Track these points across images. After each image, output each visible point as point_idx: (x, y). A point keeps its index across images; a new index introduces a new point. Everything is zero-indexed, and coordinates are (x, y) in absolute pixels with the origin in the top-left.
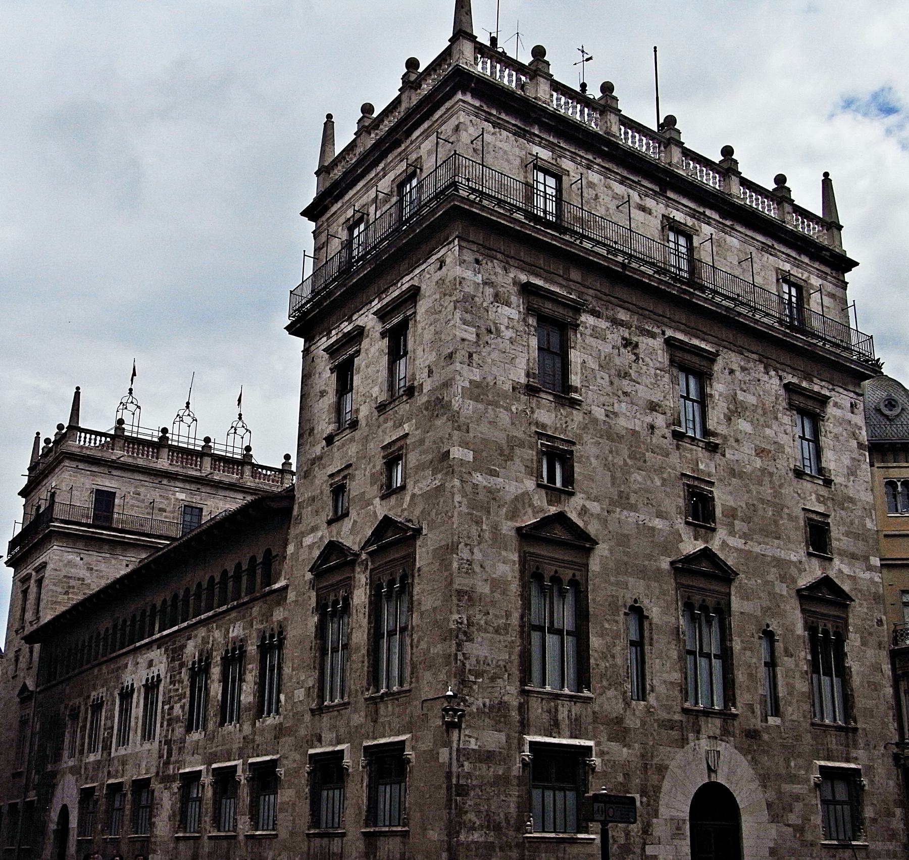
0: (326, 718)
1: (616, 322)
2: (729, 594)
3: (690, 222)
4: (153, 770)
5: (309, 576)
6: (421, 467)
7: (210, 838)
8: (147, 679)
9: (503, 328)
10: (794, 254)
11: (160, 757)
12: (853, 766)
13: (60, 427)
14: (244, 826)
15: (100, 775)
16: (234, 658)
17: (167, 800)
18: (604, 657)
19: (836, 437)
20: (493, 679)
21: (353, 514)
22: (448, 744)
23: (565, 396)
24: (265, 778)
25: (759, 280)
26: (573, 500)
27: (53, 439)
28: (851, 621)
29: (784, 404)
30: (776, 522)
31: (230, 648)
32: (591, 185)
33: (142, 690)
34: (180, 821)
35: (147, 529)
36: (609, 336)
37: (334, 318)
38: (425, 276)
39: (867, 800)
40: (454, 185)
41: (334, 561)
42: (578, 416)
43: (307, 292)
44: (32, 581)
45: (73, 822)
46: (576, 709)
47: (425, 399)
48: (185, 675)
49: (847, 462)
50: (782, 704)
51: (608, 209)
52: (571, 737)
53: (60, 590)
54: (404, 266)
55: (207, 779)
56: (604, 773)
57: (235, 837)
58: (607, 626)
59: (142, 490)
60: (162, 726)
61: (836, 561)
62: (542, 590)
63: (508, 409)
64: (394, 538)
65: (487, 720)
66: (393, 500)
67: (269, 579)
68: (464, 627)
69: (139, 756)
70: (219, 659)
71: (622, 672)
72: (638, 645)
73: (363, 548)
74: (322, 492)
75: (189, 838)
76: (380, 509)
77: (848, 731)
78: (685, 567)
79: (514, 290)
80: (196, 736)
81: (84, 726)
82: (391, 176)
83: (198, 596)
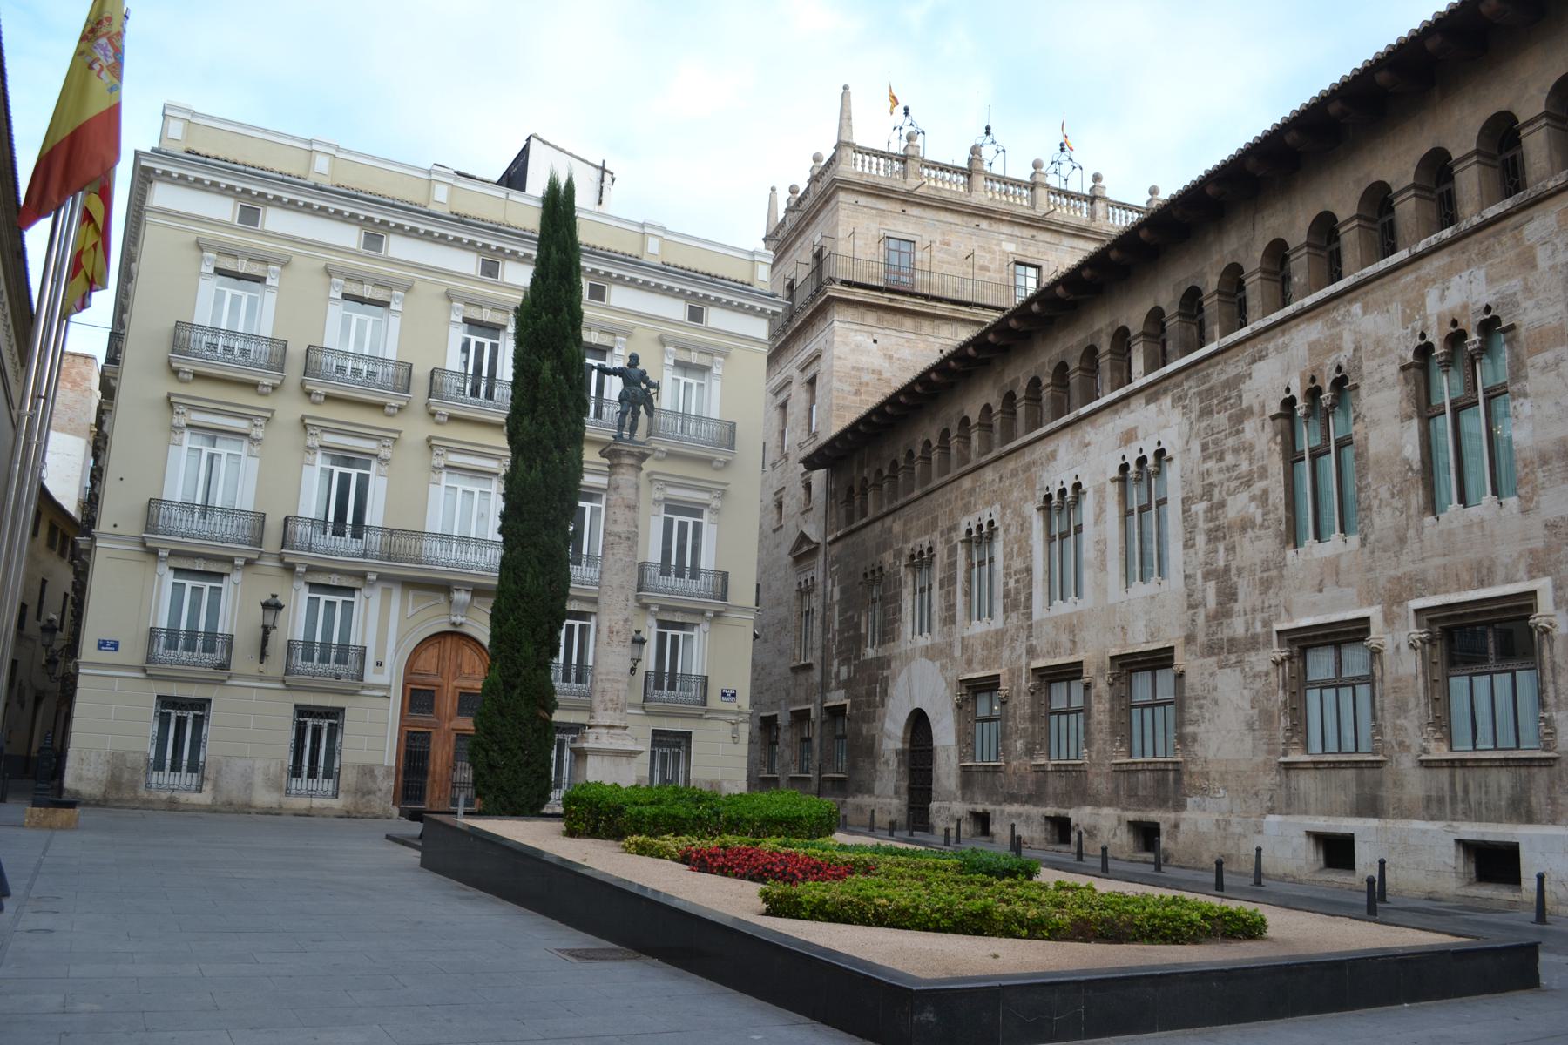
7: (1427, 765)
8: (1124, 468)
11: (1191, 607)
13: (817, 158)
15: (1006, 653)
27: (803, 187)
31: (1435, 338)
33: (1113, 491)
34: (1293, 728)
44: (794, 387)
45: (944, 734)
53: (847, 388)
60: (1188, 544)
69: (1109, 609)
70: (1391, 371)
81: (949, 581)
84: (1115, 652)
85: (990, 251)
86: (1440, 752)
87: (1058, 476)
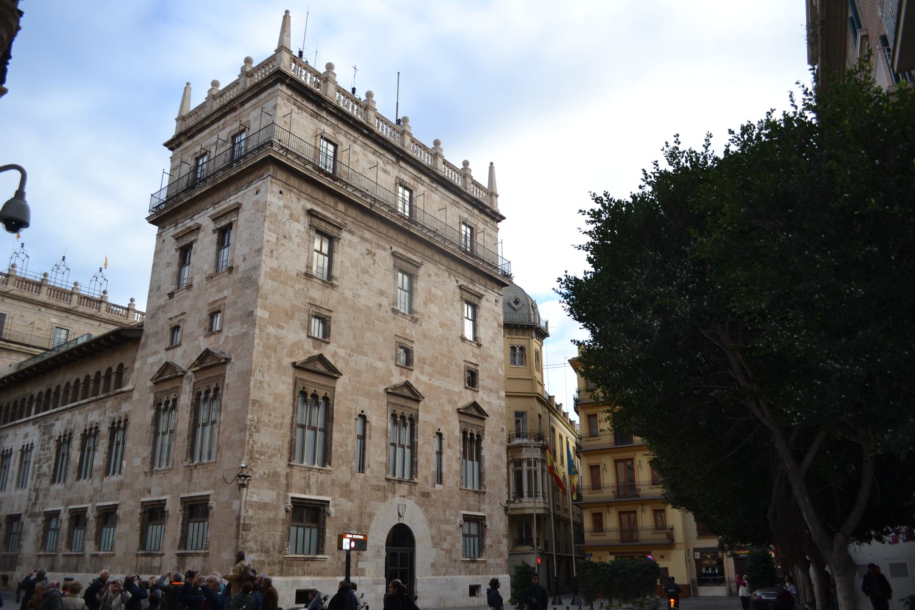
0: (155, 478)
1: (363, 239)
2: (418, 410)
3: (412, 182)
4: (23, 509)
5: (150, 384)
6: (233, 319)
7: (64, 556)
9: (293, 236)
10: (470, 208)
12: (481, 514)
14: (90, 548)
16: (90, 434)
17: (32, 529)
18: (341, 446)
19: (486, 319)
20: (271, 457)
21: (184, 345)
22: (239, 498)
23: (329, 280)
24: (108, 516)
25: (449, 222)
26: (329, 346)
28: (486, 428)
29: (458, 297)
30: (448, 368)
32: (355, 153)
33: (19, 453)
34: (42, 544)
35: (27, 342)
36: (359, 247)
37: (181, 216)
38: (245, 197)
39: (487, 534)
40: (271, 143)
41: (167, 375)
42: (334, 295)
43: (163, 196)
46: (322, 477)
47: (239, 276)
48: (53, 445)
49: (491, 334)
50: (444, 477)
51: (364, 169)
52: (318, 494)
54: (233, 188)
55: (65, 516)
56: (336, 517)
57: (83, 555)
58: (344, 426)
59: (26, 314)
61: (481, 392)
62: (305, 401)
63: (293, 287)
64: (211, 363)
65: (266, 483)
66: (213, 338)
67: (119, 384)
68: (255, 423)
70: (79, 435)
71: (351, 455)
72: (363, 438)
73: (190, 368)
74: (163, 329)
75: (48, 556)
76: (204, 343)
77: (480, 493)
78: (392, 392)
79: (303, 213)
80: (58, 486)
82: (228, 130)
83: (66, 392)
84: (9, 513)
85: (44, 322)
86: (68, 552)
87: (7, 444)
